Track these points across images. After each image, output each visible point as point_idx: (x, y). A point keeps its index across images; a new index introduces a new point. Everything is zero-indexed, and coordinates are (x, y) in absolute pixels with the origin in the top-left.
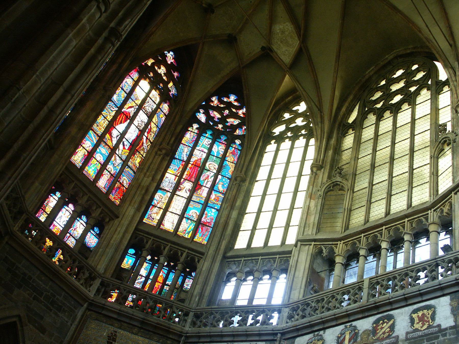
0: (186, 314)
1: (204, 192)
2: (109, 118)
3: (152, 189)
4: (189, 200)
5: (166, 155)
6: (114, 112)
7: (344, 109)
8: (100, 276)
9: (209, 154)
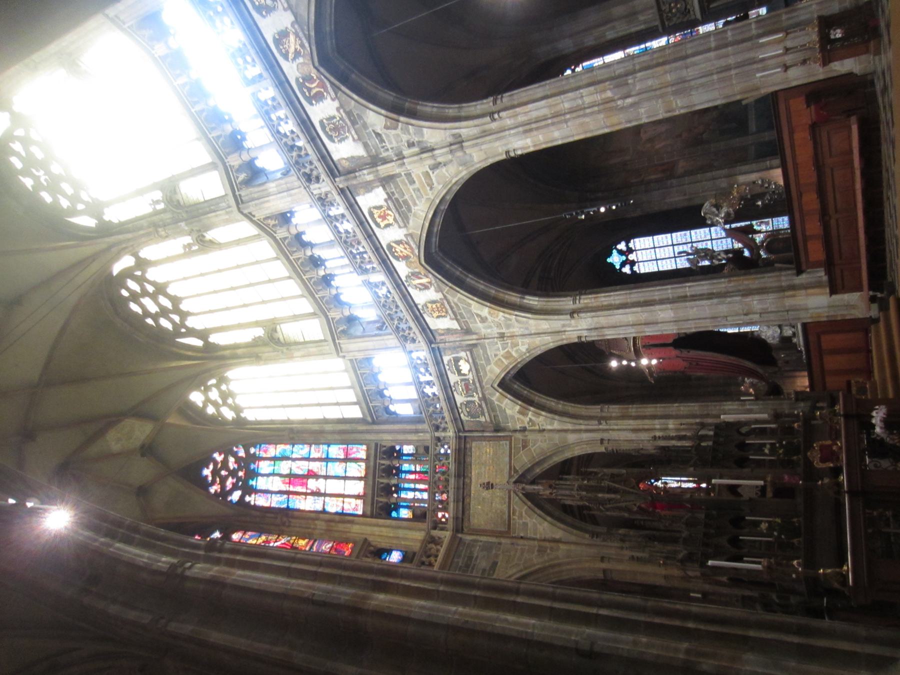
0: (438, 439)
1: (315, 466)
3: (327, 517)
4: (326, 477)
5: (287, 516)
7: (190, 353)
8: (428, 533)
9: (273, 474)
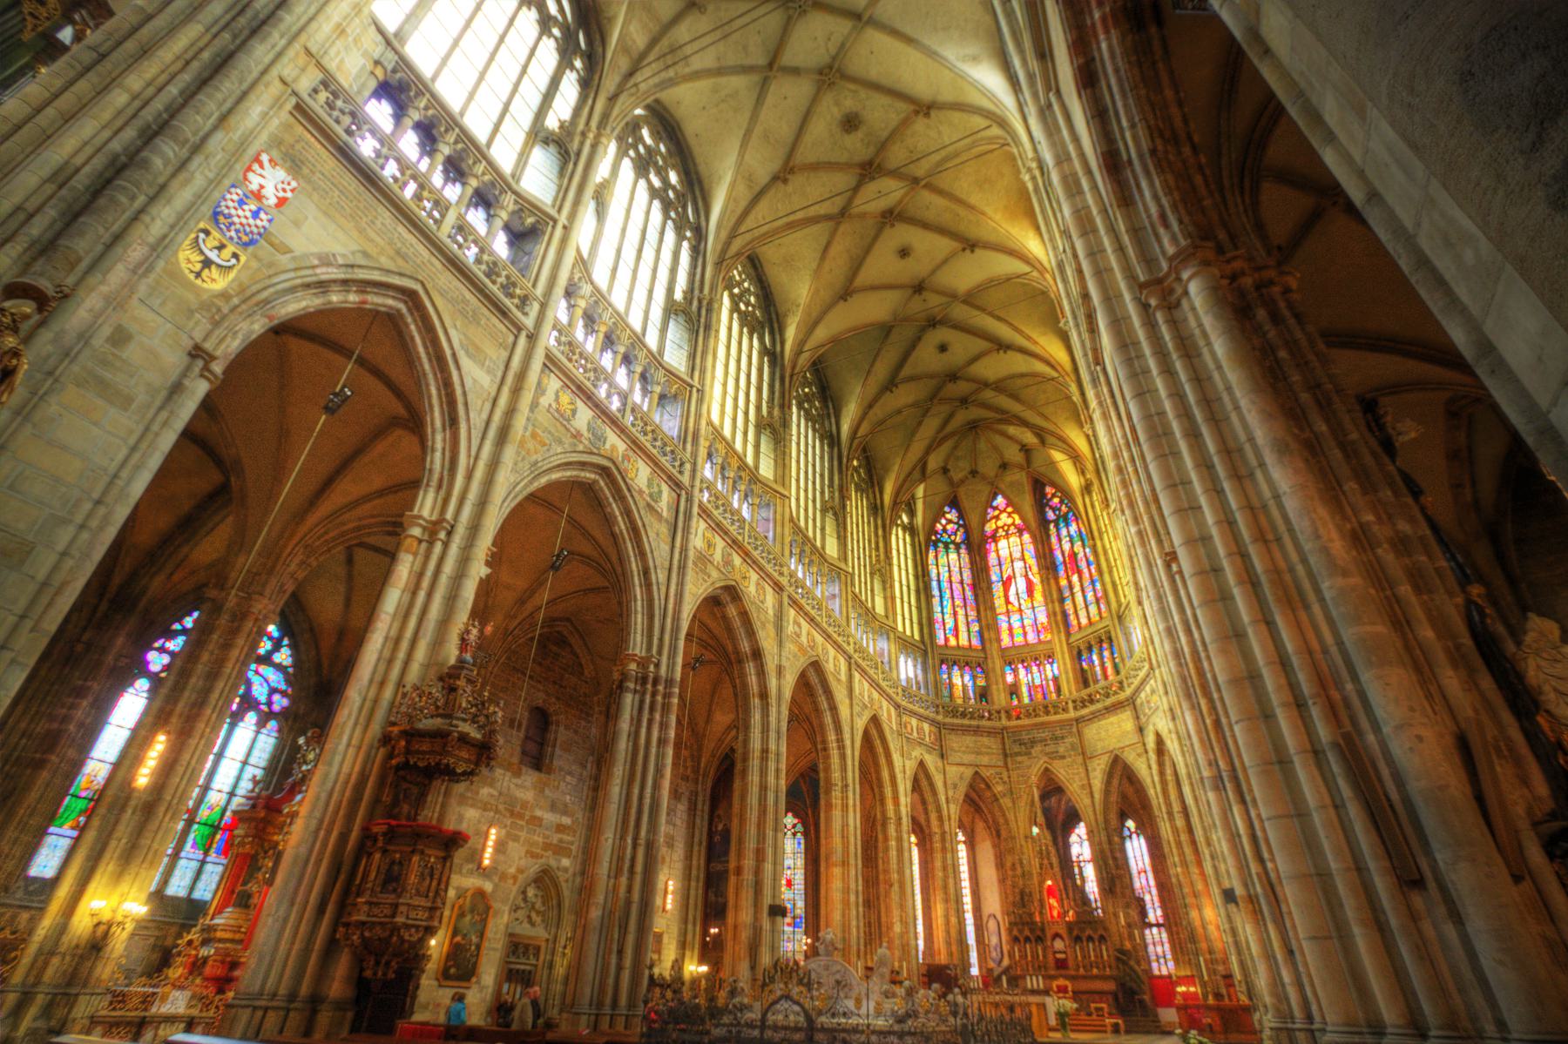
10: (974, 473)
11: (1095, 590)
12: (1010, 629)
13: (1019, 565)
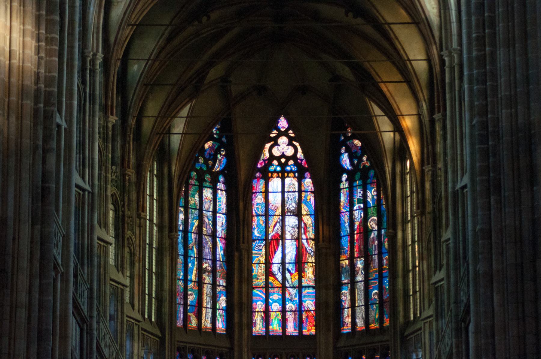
2: (263, 260)
6: (264, 249)
10: (261, 90)
11: (381, 288)
12: (267, 312)
13: (291, 221)
